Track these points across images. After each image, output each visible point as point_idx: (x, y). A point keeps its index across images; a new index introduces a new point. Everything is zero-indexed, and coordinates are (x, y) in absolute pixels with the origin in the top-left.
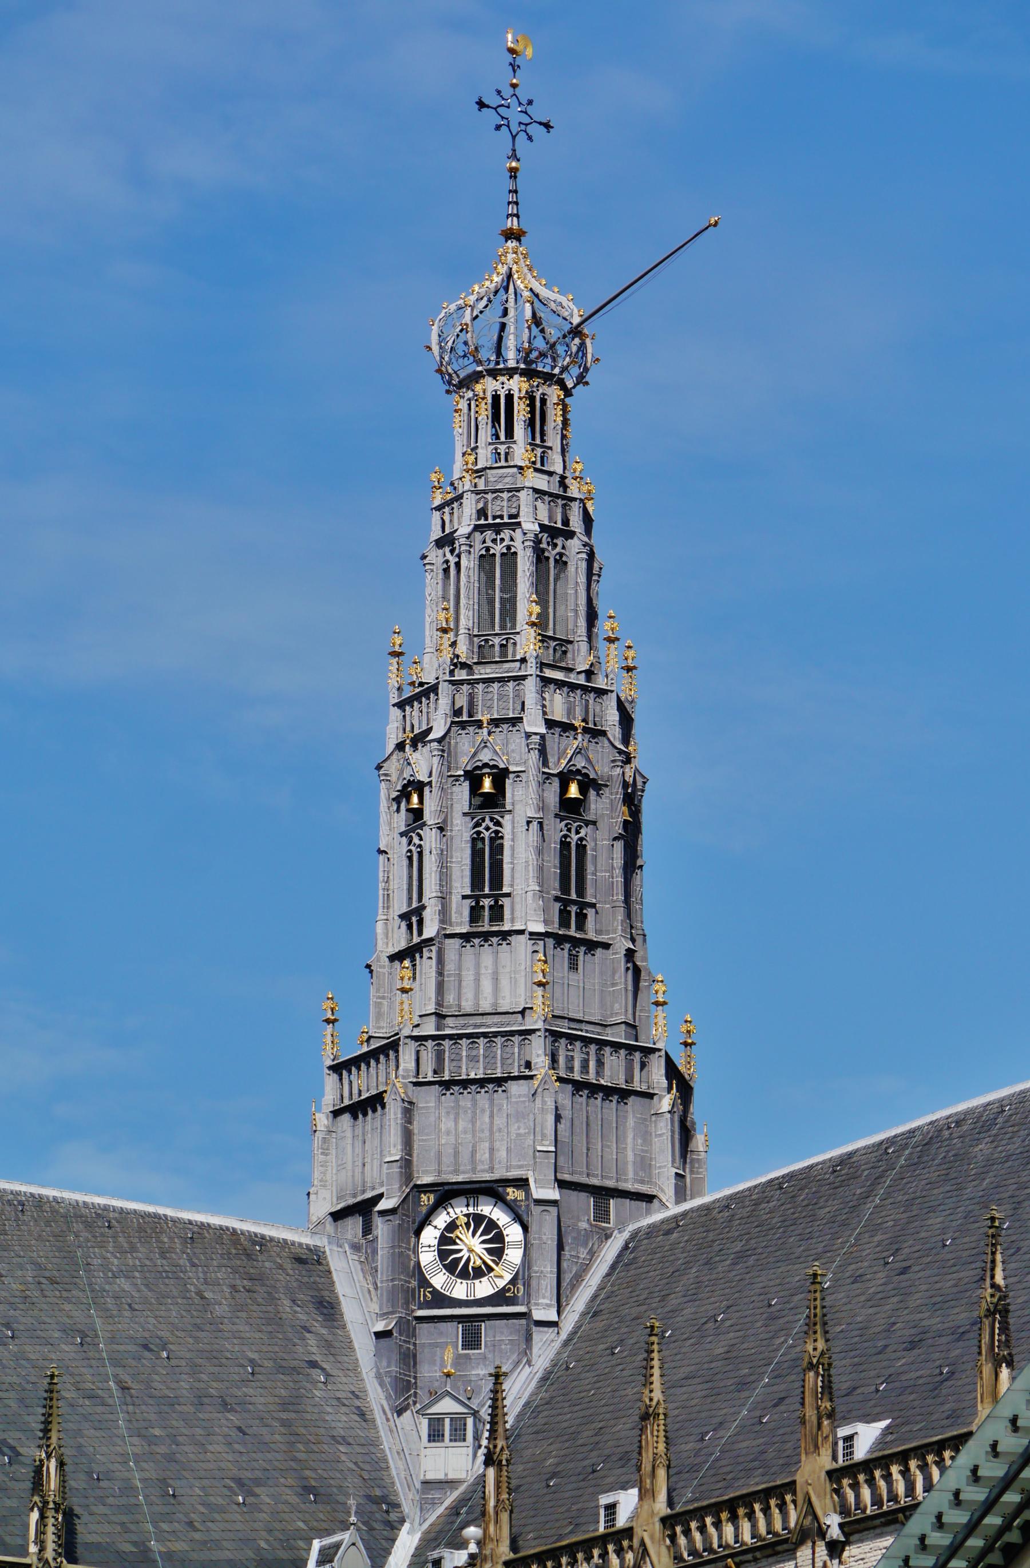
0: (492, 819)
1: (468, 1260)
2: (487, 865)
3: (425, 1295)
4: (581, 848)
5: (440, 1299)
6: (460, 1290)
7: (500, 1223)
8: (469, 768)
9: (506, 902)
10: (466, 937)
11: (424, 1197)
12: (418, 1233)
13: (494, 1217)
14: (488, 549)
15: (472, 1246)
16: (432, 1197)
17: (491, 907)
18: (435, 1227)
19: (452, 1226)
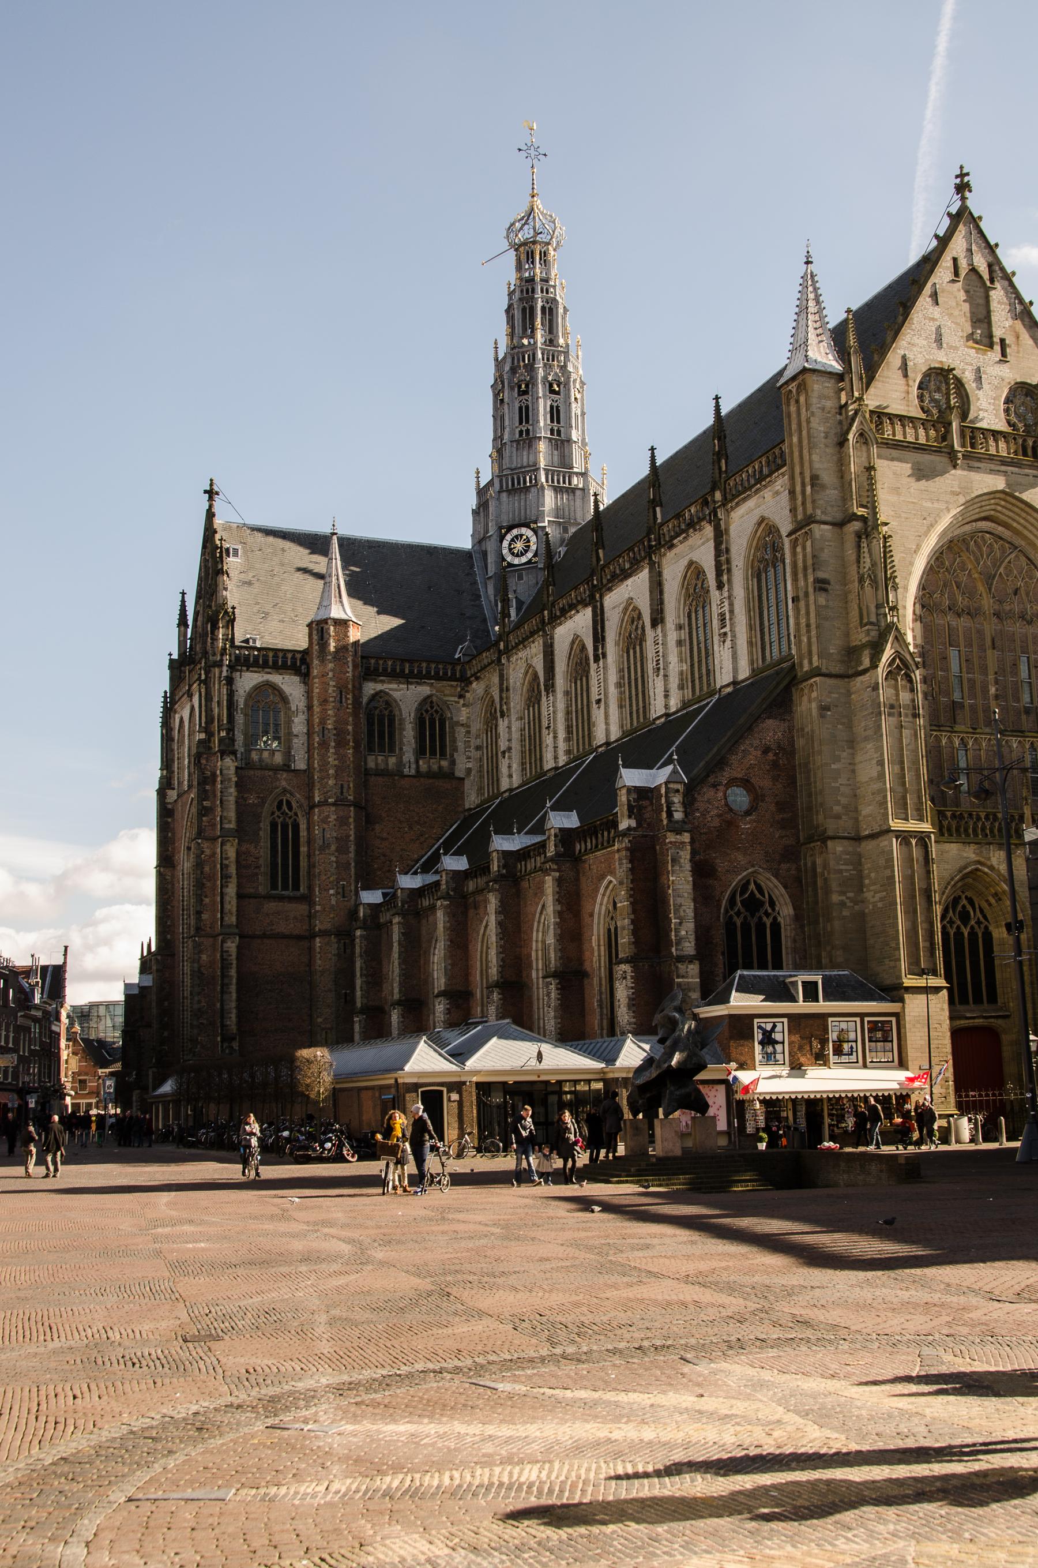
2: (526, 415)
4: (557, 407)
5: (510, 565)
6: (516, 561)
10: (518, 442)
12: (501, 542)
15: (519, 546)
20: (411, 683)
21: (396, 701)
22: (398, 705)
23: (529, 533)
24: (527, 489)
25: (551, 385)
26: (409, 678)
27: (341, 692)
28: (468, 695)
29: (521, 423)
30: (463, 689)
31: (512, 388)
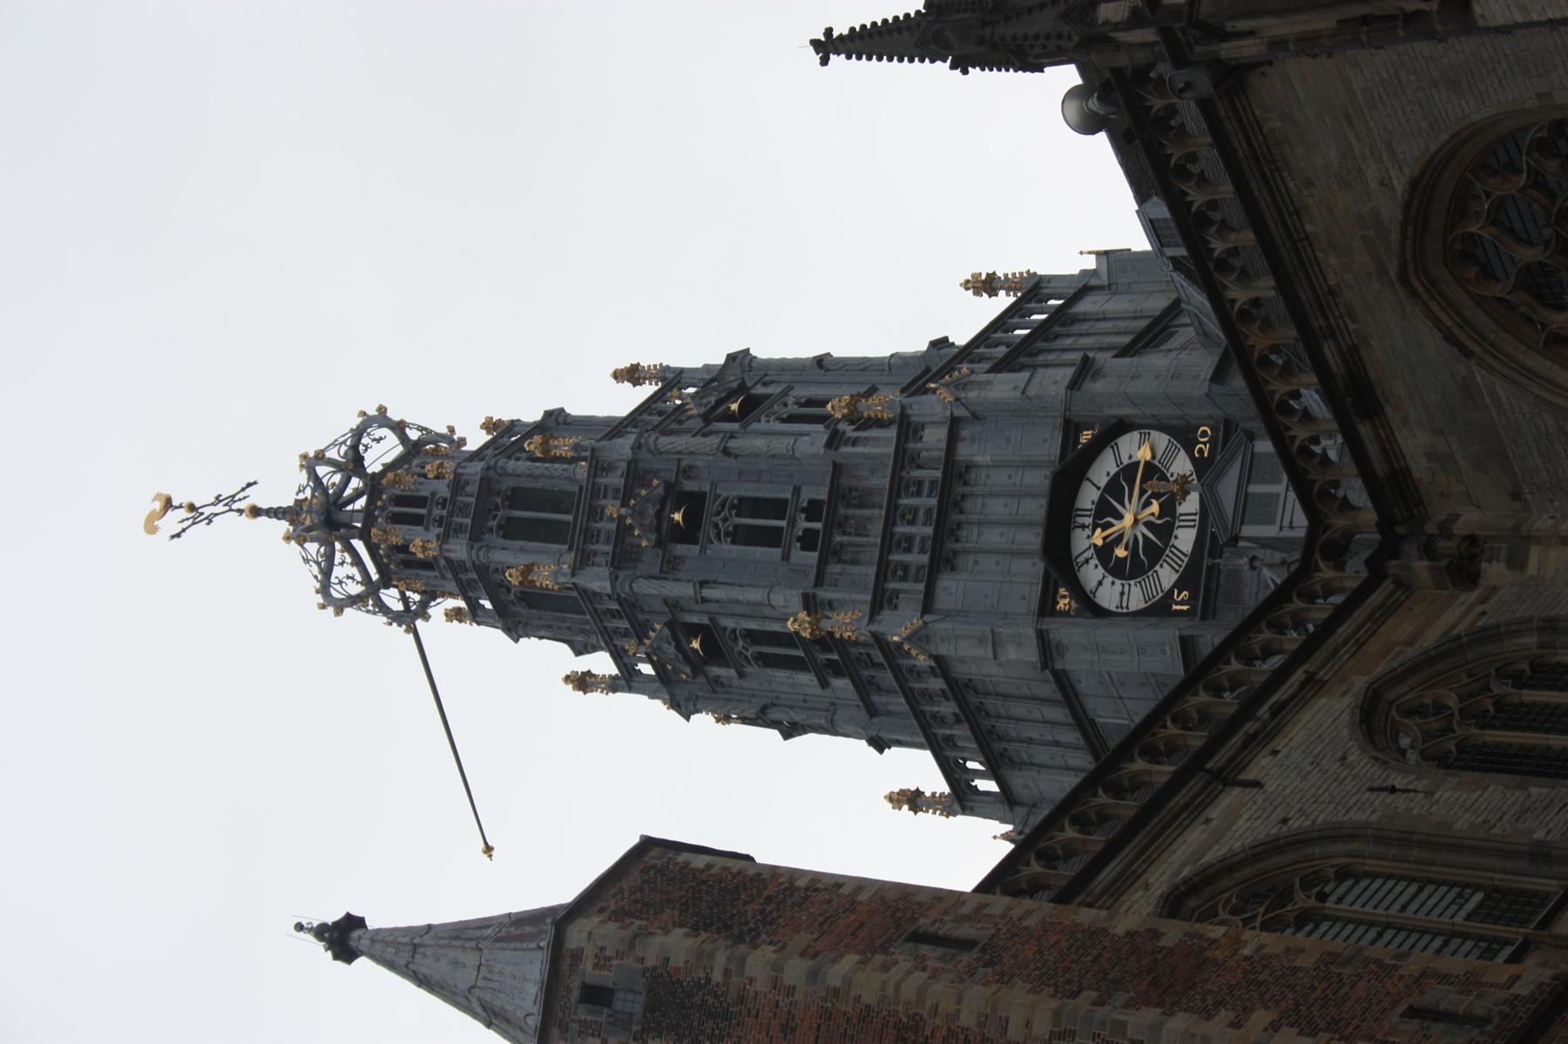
0: (718, 514)
1: (1148, 525)
2: (760, 521)
3: (1181, 603)
4: (810, 403)
6: (1185, 539)
7: (1114, 470)
8: (653, 537)
9: (807, 494)
11: (1063, 604)
13: (1103, 481)
14: (500, 527)
15: (1130, 519)
16: (1062, 591)
17: (808, 519)
18: (1100, 583)
19: (1104, 553)
20: (1239, 761)
21: (1272, 847)
22: (1299, 841)
23: (1104, 469)
24: (955, 472)
25: (729, 417)
26: (1211, 773)
27: (920, 938)
28: (1469, 519)
29: (770, 538)
30: (1429, 552)
31: (670, 567)
